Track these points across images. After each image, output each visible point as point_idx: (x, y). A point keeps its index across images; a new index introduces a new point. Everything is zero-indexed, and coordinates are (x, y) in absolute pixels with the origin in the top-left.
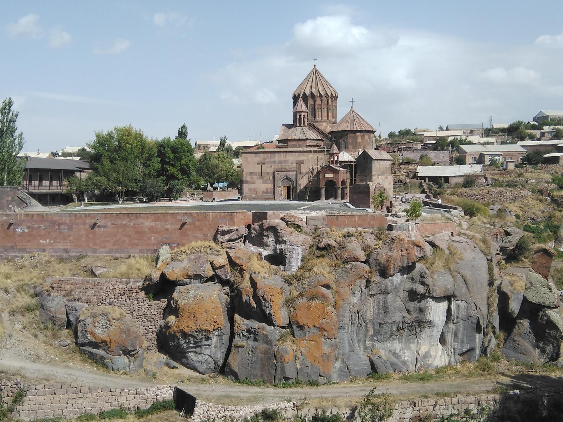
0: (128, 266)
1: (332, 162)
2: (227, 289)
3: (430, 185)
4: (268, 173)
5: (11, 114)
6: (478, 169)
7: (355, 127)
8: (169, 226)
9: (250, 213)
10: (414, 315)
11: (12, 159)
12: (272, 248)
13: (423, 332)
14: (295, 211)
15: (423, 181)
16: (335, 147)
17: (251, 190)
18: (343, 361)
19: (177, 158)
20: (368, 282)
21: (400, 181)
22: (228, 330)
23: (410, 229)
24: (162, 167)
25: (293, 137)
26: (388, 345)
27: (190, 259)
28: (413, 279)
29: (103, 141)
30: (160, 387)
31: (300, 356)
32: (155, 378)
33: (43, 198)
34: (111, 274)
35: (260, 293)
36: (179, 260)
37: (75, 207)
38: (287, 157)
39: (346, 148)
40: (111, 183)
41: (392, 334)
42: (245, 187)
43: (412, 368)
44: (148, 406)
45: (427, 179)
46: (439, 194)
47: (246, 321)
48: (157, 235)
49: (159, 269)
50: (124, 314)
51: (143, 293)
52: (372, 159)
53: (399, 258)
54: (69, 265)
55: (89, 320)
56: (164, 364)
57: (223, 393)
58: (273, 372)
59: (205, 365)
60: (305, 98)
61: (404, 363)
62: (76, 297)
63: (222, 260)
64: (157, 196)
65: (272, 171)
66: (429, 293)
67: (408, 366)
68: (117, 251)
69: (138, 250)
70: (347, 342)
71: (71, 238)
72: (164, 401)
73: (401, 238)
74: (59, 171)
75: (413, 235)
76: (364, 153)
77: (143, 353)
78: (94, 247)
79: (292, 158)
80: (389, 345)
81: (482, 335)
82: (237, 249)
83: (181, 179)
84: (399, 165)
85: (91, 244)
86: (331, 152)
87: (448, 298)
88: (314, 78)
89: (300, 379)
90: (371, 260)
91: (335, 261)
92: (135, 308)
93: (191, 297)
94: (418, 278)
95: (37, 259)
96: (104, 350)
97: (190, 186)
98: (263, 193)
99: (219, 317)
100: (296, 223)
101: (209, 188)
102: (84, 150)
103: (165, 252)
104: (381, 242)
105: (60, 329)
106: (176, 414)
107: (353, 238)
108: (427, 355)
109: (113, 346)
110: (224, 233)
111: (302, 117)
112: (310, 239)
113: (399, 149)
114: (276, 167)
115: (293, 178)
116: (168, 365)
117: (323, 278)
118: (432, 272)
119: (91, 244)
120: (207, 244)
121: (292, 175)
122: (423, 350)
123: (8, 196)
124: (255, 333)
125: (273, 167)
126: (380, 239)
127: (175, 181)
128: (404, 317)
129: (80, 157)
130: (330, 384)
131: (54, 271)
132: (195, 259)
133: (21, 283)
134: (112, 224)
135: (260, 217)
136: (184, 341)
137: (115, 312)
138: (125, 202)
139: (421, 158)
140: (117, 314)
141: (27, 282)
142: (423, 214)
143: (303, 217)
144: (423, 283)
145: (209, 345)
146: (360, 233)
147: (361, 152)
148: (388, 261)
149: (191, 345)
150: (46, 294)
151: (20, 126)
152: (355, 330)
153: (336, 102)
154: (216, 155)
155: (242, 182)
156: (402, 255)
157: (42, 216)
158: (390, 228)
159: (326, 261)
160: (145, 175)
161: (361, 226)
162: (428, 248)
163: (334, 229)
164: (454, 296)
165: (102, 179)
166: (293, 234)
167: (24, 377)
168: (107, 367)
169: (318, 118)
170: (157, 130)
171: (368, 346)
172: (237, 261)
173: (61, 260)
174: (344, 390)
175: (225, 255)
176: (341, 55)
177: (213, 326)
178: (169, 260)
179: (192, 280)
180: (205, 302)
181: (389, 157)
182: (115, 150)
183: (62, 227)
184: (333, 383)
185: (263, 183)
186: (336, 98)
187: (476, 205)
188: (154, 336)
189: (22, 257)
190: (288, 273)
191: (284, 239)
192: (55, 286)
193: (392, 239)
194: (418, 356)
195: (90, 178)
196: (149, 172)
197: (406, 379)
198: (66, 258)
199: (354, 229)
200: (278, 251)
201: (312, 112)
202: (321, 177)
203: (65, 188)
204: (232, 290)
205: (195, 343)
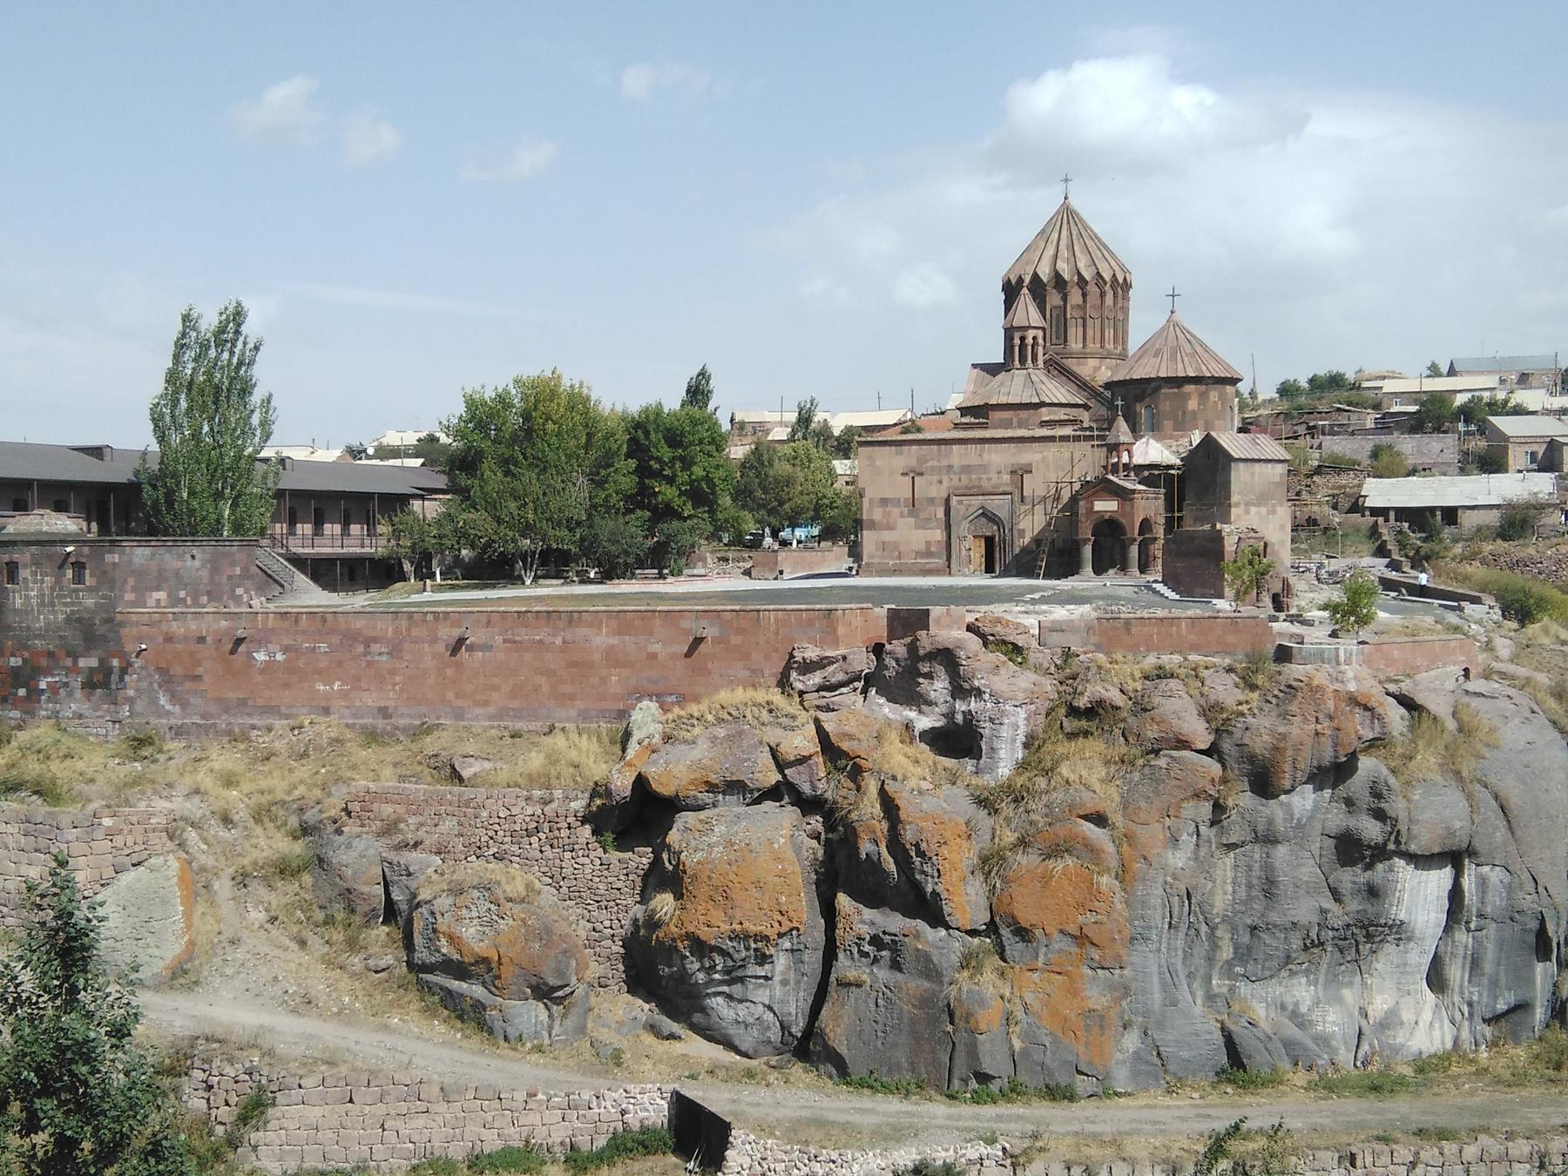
0: (548, 757)
1: (1115, 469)
2: (816, 822)
3: (1400, 532)
4: (932, 501)
5: (240, 344)
6: (1543, 485)
7: (1180, 366)
8: (656, 648)
9: (881, 612)
10: (1354, 905)
11: (244, 466)
12: (943, 709)
13: (1381, 955)
14: (1007, 606)
15: (1381, 519)
16: (1122, 425)
17: (884, 546)
18: (1146, 1034)
19: (682, 459)
20: (1219, 808)
21: (1312, 522)
22: (820, 938)
23: (1342, 659)
24: (641, 483)
25: (1003, 400)
26: (1275, 989)
27: (714, 740)
28: (1349, 802)
29: (482, 417)
30: (634, 1089)
31: (1019, 1014)
32: (619, 1065)
33: (323, 571)
34: (503, 777)
35: (909, 835)
36: (685, 741)
37: (407, 595)
38: (986, 456)
39: (1155, 429)
40: (503, 530)
41: (1288, 959)
42: (869, 539)
43: (1345, 1057)
44: (601, 1142)
45: (1392, 515)
46: (1427, 558)
47: (868, 913)
48: (625, 672)
49: (630, 765)
50: (537, 885)
51: (587, 829)
53: (1309, 741)
54: (394, 752)
55: (444, 902)
56: (644, 1027)
57: (805, 1113)
58: (943, 1055)
59: (756, 1033)
60: (1038, 289)
61: (1324, 1041)
62: (411, 838)
63: (801, 741)
64: (626, 564)
66: (1397, 842)
67: (1334, 1051)
68: (518, 715)
69: (573, 713)
70: (1156, 979)
71: (398, 679)
72: (644, 1130)
73: (1316, 682)
74: (366, 497)
75: (1350, 674)
76: (1209, 444)
77: (587, 996)
78: (459, 702)
79: (999, 458)
80: (1279, 990)
81: (1552, 966)
82: (843, 712)
83: (690, 517)
84: (1311, 476)
85: (450, 696)
86: (1111, 440)
87: (1455, 858)
88: (1065, 233)
89: (1022, 1078)
90: (1226, 745)
91: (1121, 748)
92: (568, 871)
93: (717, 844)
94: (1365, 799)
95: (309, 733)
96: (484, 984)
97: (714, 536)
98: (918, 554)
99: (794, 898)
100: (1011, 639)
101: (768, 541)
102: (432, 439)
103: (647, 719)
104: (1255, 695)
105: (367, 924)
106: (676, 1166)
107: (1173, 683)
108: (1389, 1021)
109: (507, 972)
110: (808, 667)
111: (1030, 341)
112: (1049, 686)
113: (1309, 428)
114: (956, 482)
115: (1003, 514)
116: (653, 1029)
117: (1087, 796)
118: (1408, 783)
119: (450, 696)
120: (761, 696)
122: (1380, 1004)
123: (233, 564)
124: (895, 947)
126: (1253, 687)
127: (676, 524)
128: (1323, 911)
129: (421, 461)
130: (1108, 1096)
131: (353, 768)
132: (729, 738)
133: (264, 799)
134: (505, 641)
135: (908, 621)
136: (697, 965)
137: (514, 879)
138: (541, 581)
139: (1375, 455)
140: (517, 887)
141: (280, 795)
142: (1382, 615)
143: (1031, 622)
144: (1380, 815)
145: (766, 978)
146: (1194, 670)
147: (1197, 438)
148: (1276, 749)
149: (717, 976)
150: (331, 828)
151: (266, 377)
152: (1180, 943)
153: (1126, 298)
154: (787, 449)
155: (858, 525)
156: (1317, 734)
157: (320, 617)
158: (1283, 655)
159: (1094, 747)
160: (594, 506)
161: (1196, 648)
162: (1396, 715)
163: (1119, 657)
164: (1471, 852)
165: (479, 520)
166: (1003, 671)
167: (270, 1053)
168: (491, 1032)
169: (1075, 345)
170: (628, 382)
171: (1216, 990)
172: (845, 746)
173: (372, 737)
174: (1146, 1114)
175: (813, 727)
176: (1137, 165)
177: (776, 925)
178: (657, 740)
179: (720, 797)
180: (755, 857)
182: (514, 439)
183: (375, 648)
184: (1116, 1094)
185: (917, 527)
186: (1127, 286)
187: (1538, 588)
188: (617, 948)
189: (270, 729)
190: (987, 780)
191: (977, 683)
192: (355, 807)
193: (1290, 686)
194: (1364, 1023)
195: (449, 516)
196: (606, 499)
197: (1329, 1086)
198: (384, 733)
199: (1177, 658)
200: (959, 718)
201: (1058, 328)
202: (1082, 511)
203: (382, 542)
204: (830, 826)
205: (727, 972)
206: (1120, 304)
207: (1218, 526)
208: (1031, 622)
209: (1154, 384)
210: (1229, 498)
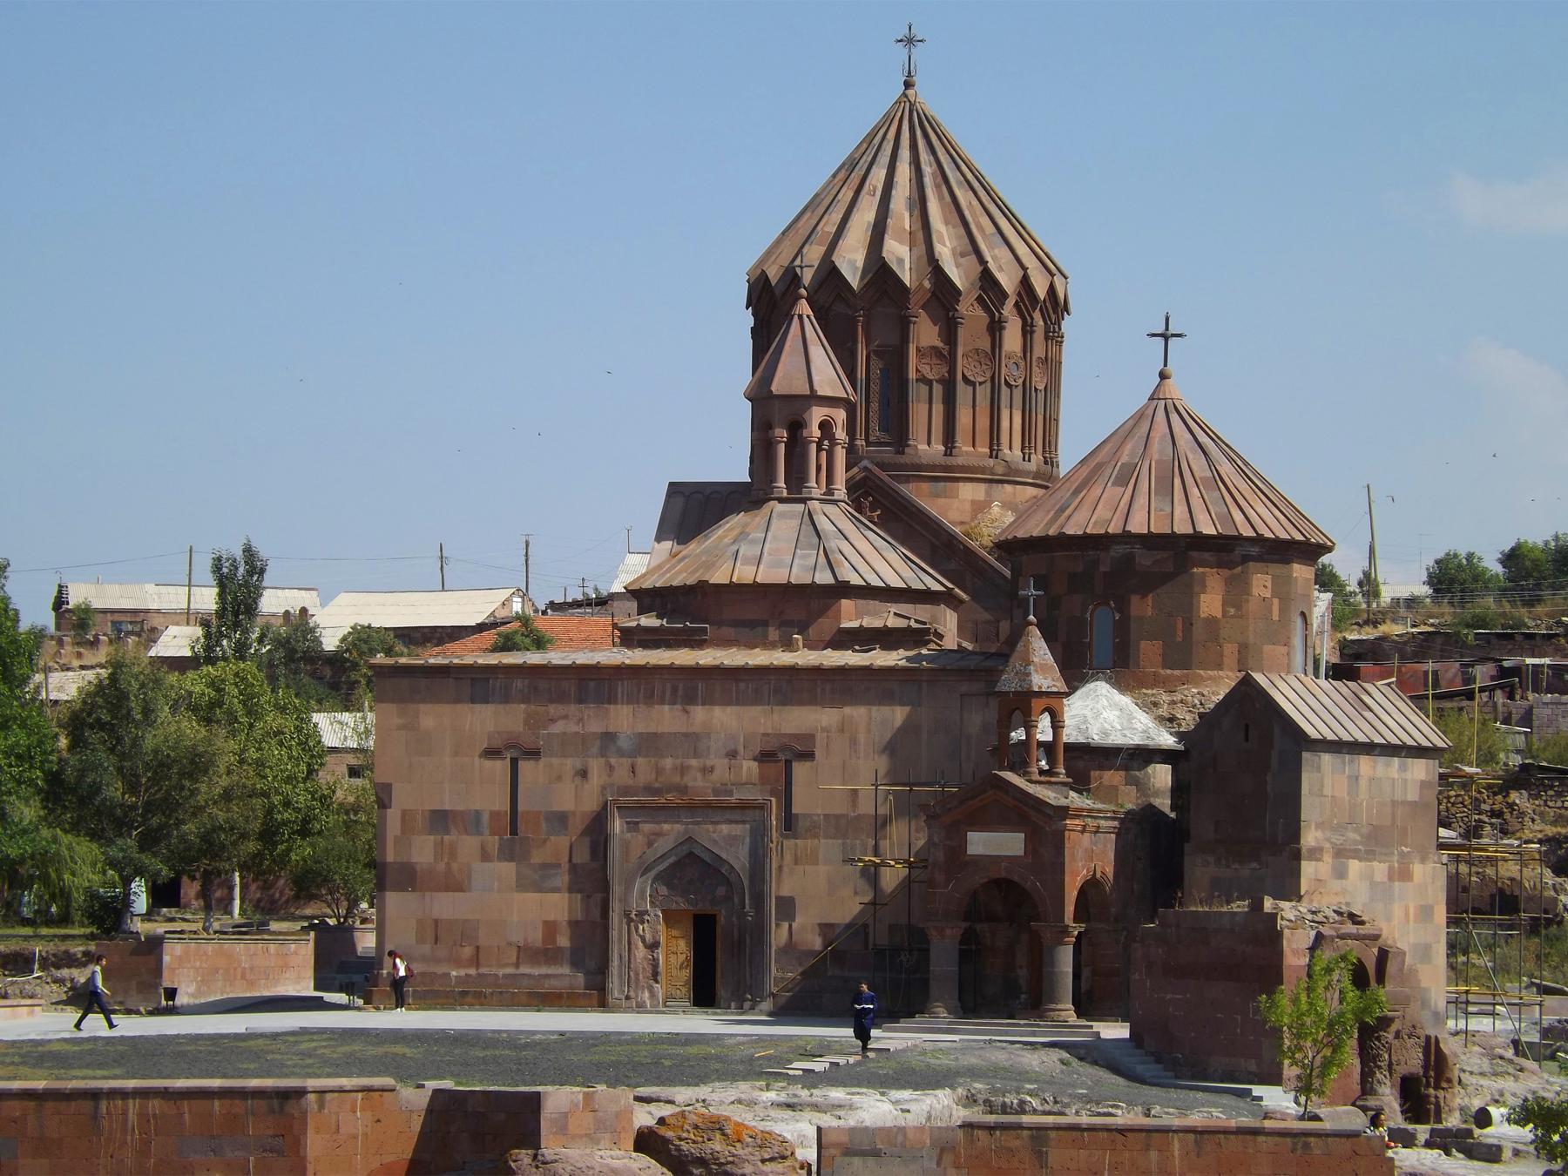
7: (1180, 510)
14: (743, 1089)
16: (1039, 649)
17: (436, 931)
65: (591, 805)
86: (1008, 682)
98: (527, 953)
114: (622, 776)
115: (738, 858)
121: (732, 840)
125: (597, 777)
143: (800, 1132)
147: (1215, 689)
153: (1054, 336)
169: (926, 448)
181: (1422, 730)
185: (523, 885)
186: (1056, 307)
206: (1039, 350)
207: (1268, 904)
208: (800, 1132)
209: (1118, 550)
210: (1295, 834)
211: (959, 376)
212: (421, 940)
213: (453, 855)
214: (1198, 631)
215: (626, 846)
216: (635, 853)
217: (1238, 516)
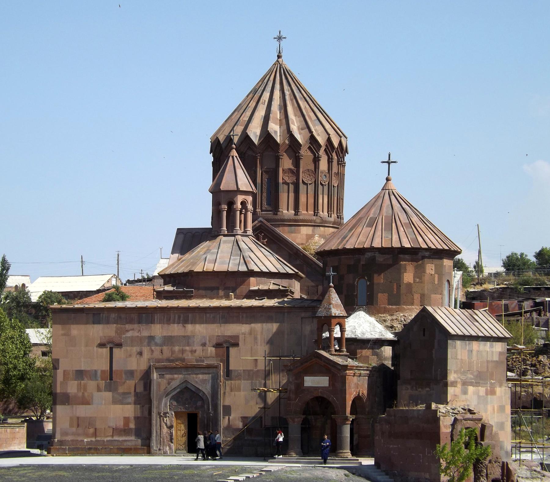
4: (131, 373)
7: (395, 236)
16: (335, 298)
17: (78, 422)
52: (446, 335)
65: (144, 367)
86: (321, 312)
88: (277, 94)
98: (117, 431)
114: (157, 354)
115: (206, 389)
121: (204, 381)
147: (410, 313)
153: (341, 163)
169: (286, 212)
181: (500, 330)
185: (115, 402)
186: (342, 151)
207: (434, 406)
209: (369, 255)
210: (445, 375)
211: (301, 181)
212: (71, 426)
213: (85, 389)
214: (403, 290)
215: (159, 385)
216: (163, 388)
217: (420, 239)
